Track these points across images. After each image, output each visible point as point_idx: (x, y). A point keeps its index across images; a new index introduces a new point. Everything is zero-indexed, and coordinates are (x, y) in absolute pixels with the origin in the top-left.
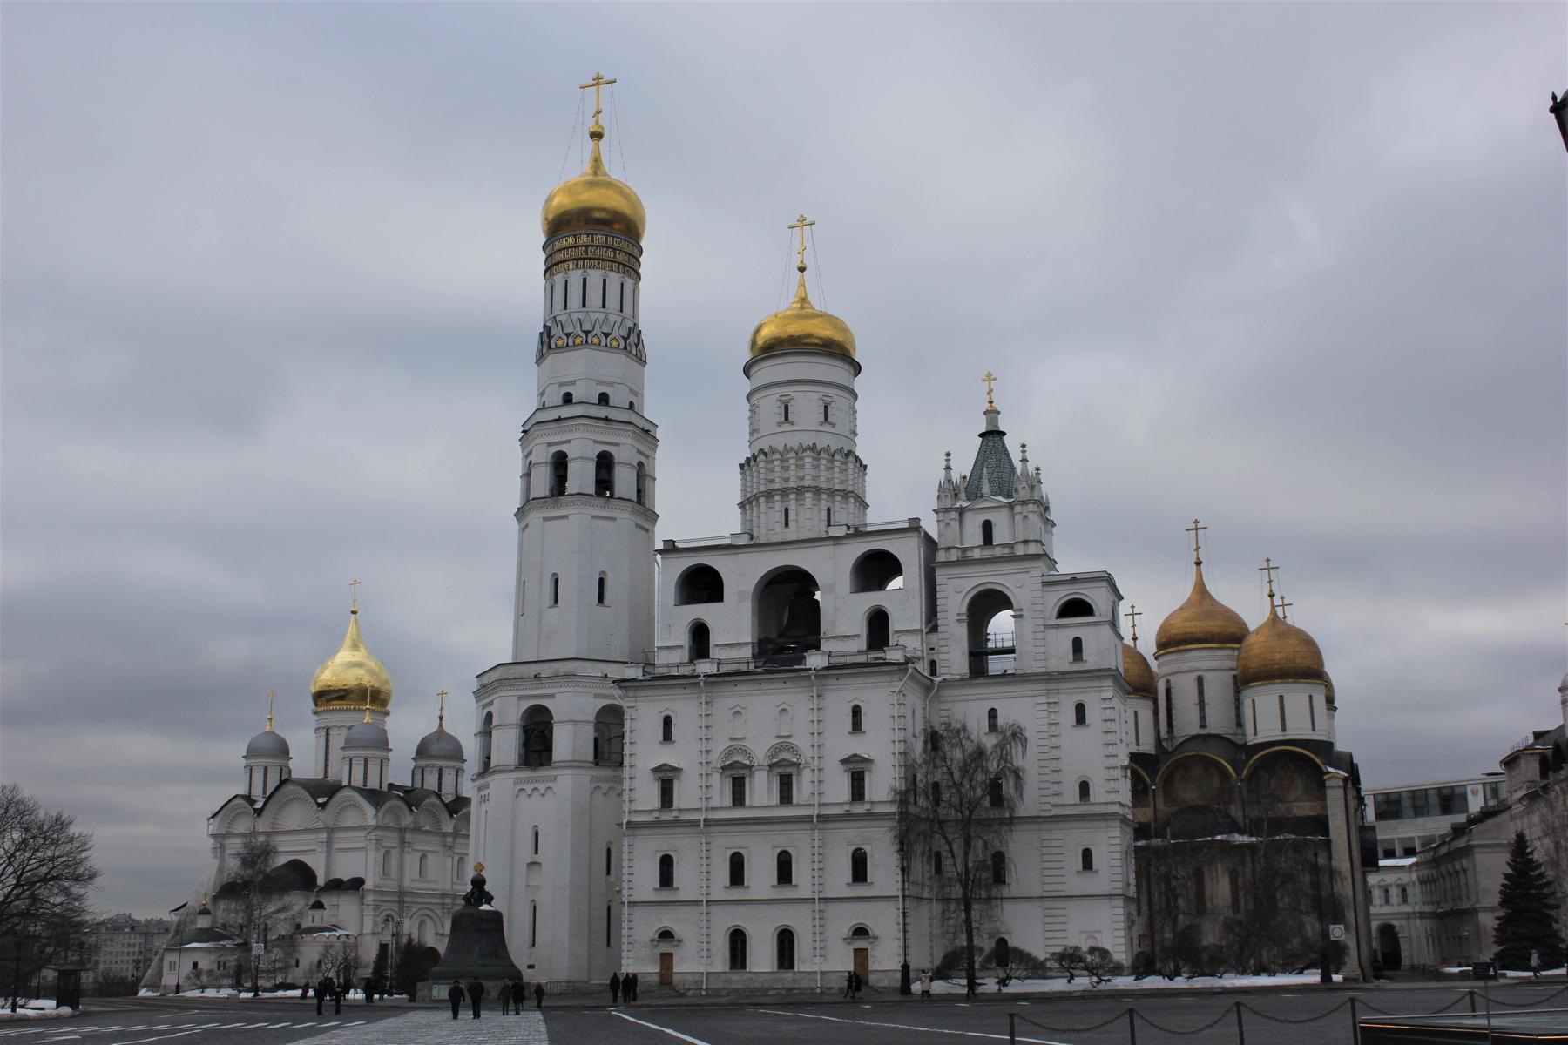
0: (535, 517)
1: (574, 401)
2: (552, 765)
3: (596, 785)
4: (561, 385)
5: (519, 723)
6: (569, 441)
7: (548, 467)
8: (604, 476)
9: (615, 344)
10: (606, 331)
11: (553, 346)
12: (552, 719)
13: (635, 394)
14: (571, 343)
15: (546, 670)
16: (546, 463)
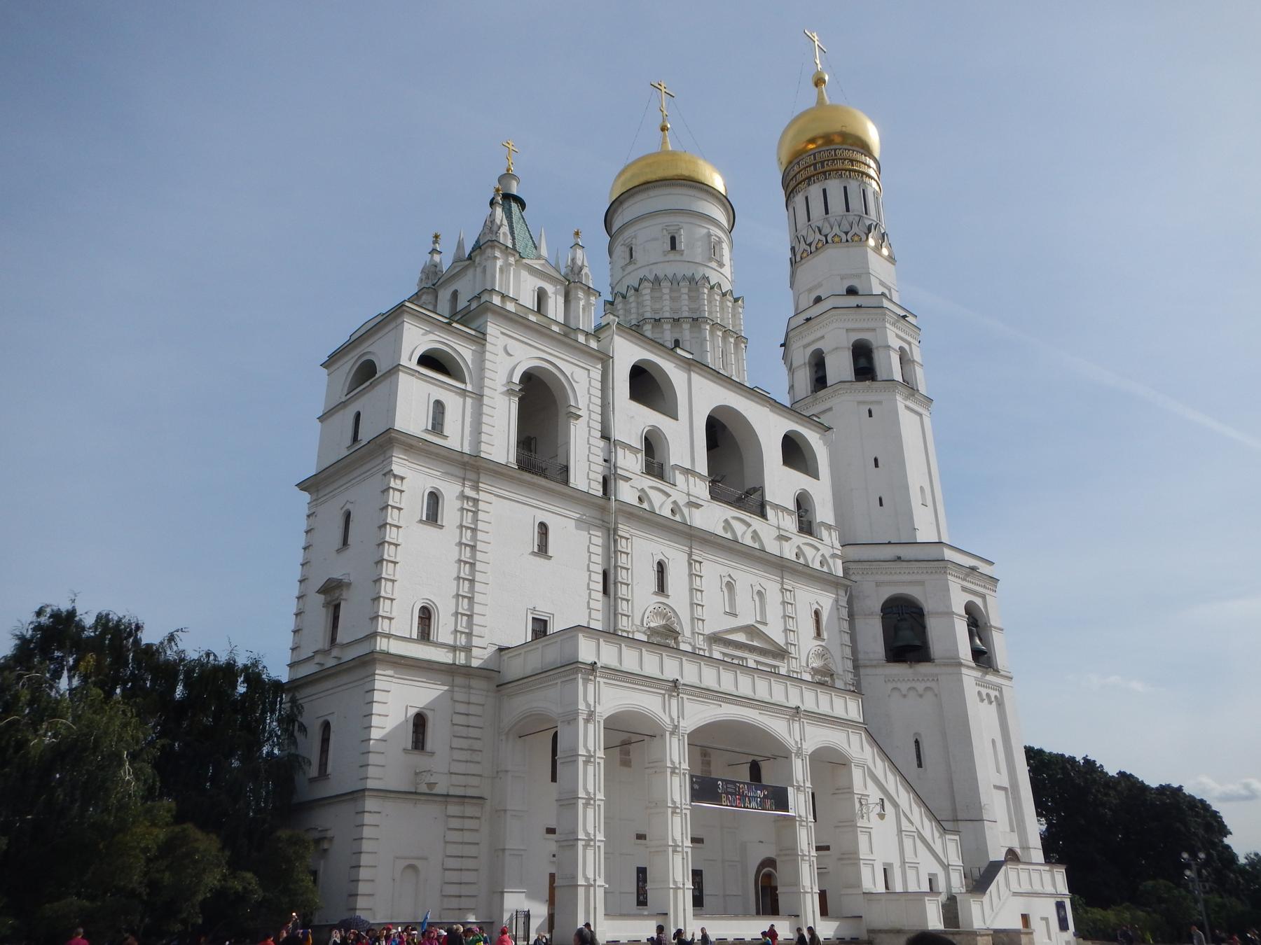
1: (860, 293)
14: (849, 239)
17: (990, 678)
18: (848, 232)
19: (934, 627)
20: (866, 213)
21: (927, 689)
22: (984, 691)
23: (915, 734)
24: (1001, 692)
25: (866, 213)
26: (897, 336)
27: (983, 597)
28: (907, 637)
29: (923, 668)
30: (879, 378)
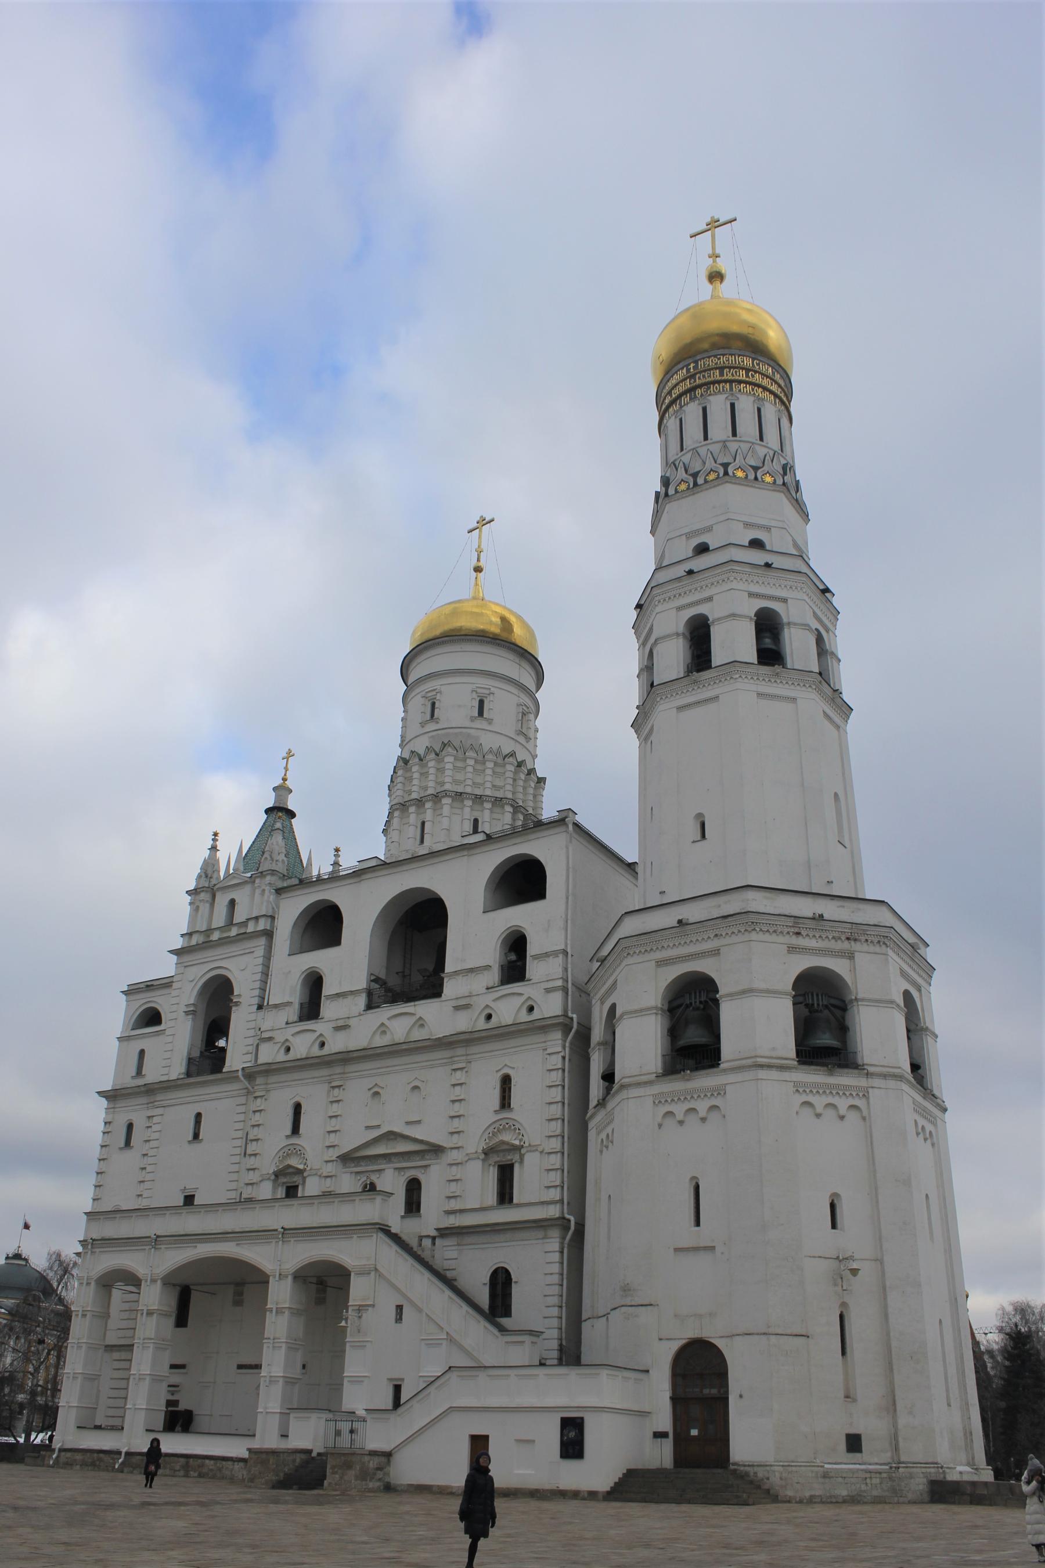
0: (664, 712)
1: (711, 549)
2: (722, 1066)
3: (804, 1098)
4: (689, 536)
5: (659, 1005)
6: (710, 599)
7: (681, 640)
8: (768, 643)
9: (768, 479)
10: (750, 464)
11: (671, 491)
12: (717, 991)
13: (796, 545)
14: (700, 481)
15: (693, 913)
16: (678, 634)
17: (845, 1079)
18: (700, 471)
19: (729, 1014)
20: (734, 434)
21: (714, 1108)
22: (819, 1101)
23: (694, 1178)
24: (868, 1099)
25: (734, 434)
26: (751, 595)
27: (851, 956)
28: (693, 1035)
29: (705, 1080)
30: (713, 666)
